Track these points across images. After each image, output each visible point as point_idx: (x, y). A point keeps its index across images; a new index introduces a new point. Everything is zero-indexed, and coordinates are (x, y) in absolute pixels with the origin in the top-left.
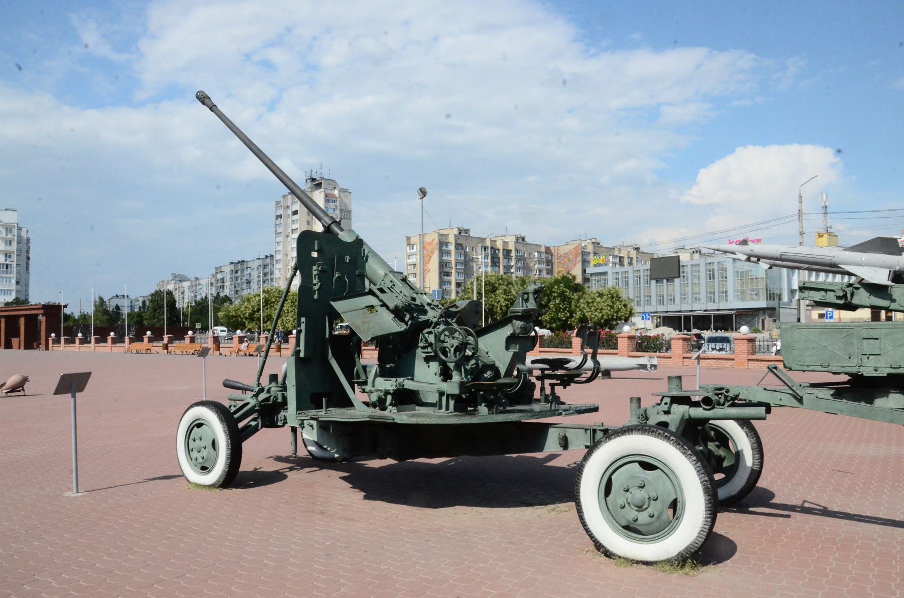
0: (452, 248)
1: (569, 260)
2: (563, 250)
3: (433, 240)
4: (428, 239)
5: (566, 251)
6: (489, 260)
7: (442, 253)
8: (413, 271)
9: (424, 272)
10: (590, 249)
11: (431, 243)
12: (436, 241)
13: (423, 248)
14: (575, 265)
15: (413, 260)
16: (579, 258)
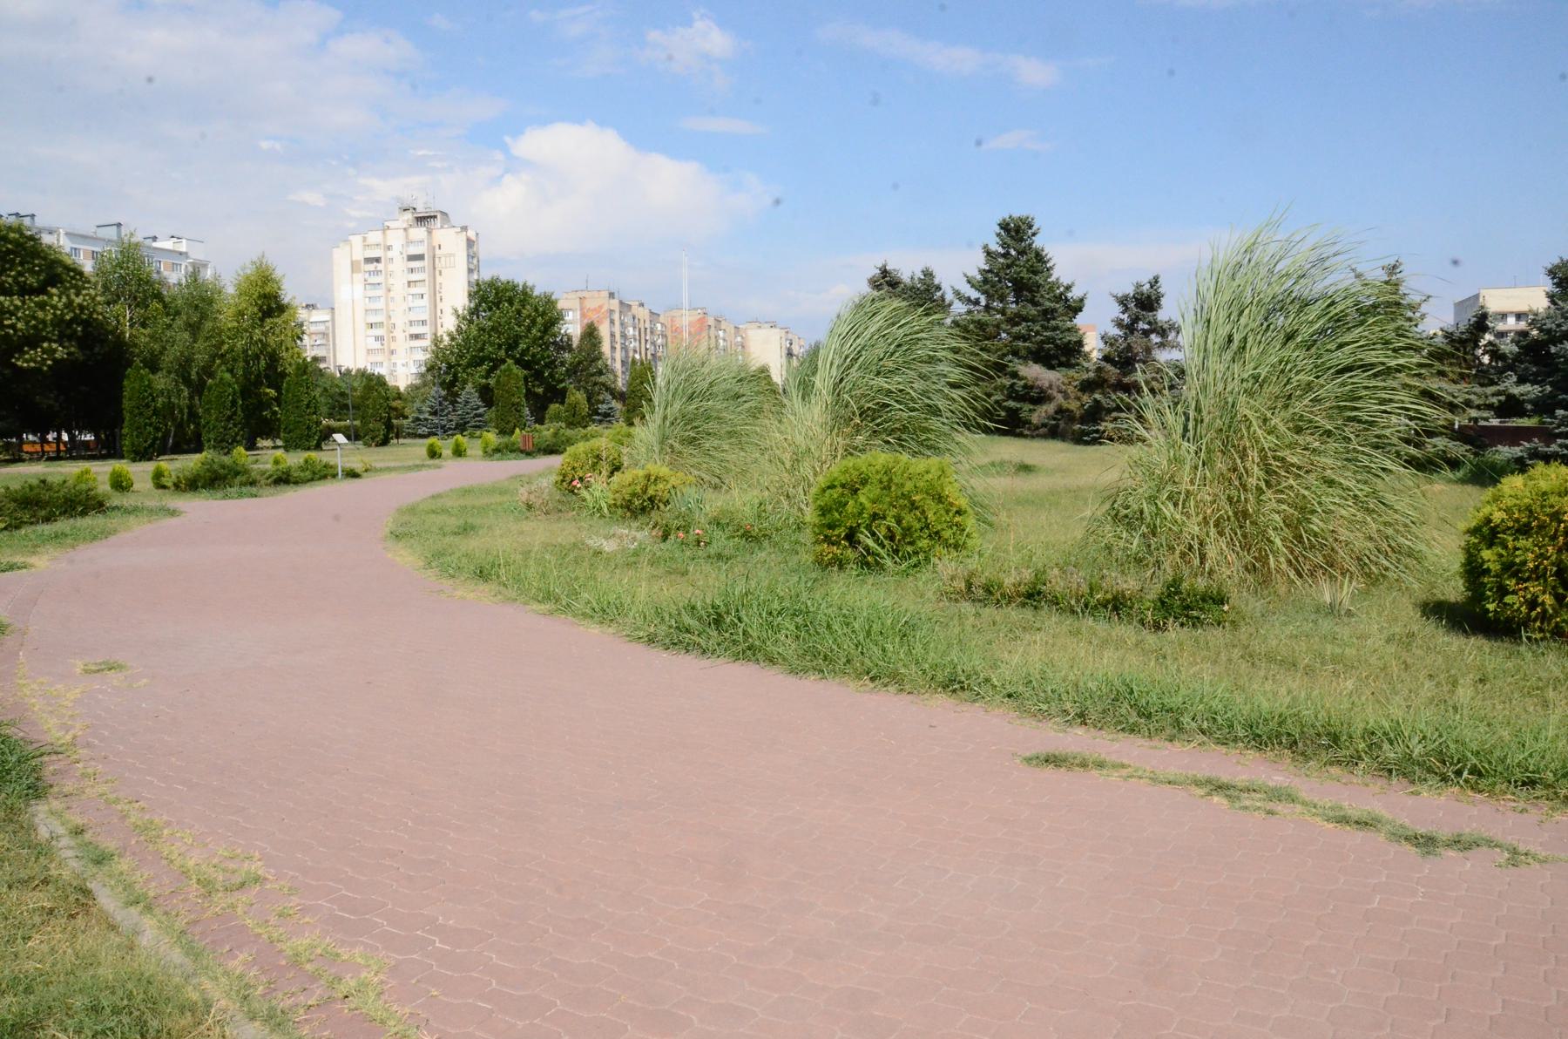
0: (616, 316)
4: (589, 304)
7: (612, 322)
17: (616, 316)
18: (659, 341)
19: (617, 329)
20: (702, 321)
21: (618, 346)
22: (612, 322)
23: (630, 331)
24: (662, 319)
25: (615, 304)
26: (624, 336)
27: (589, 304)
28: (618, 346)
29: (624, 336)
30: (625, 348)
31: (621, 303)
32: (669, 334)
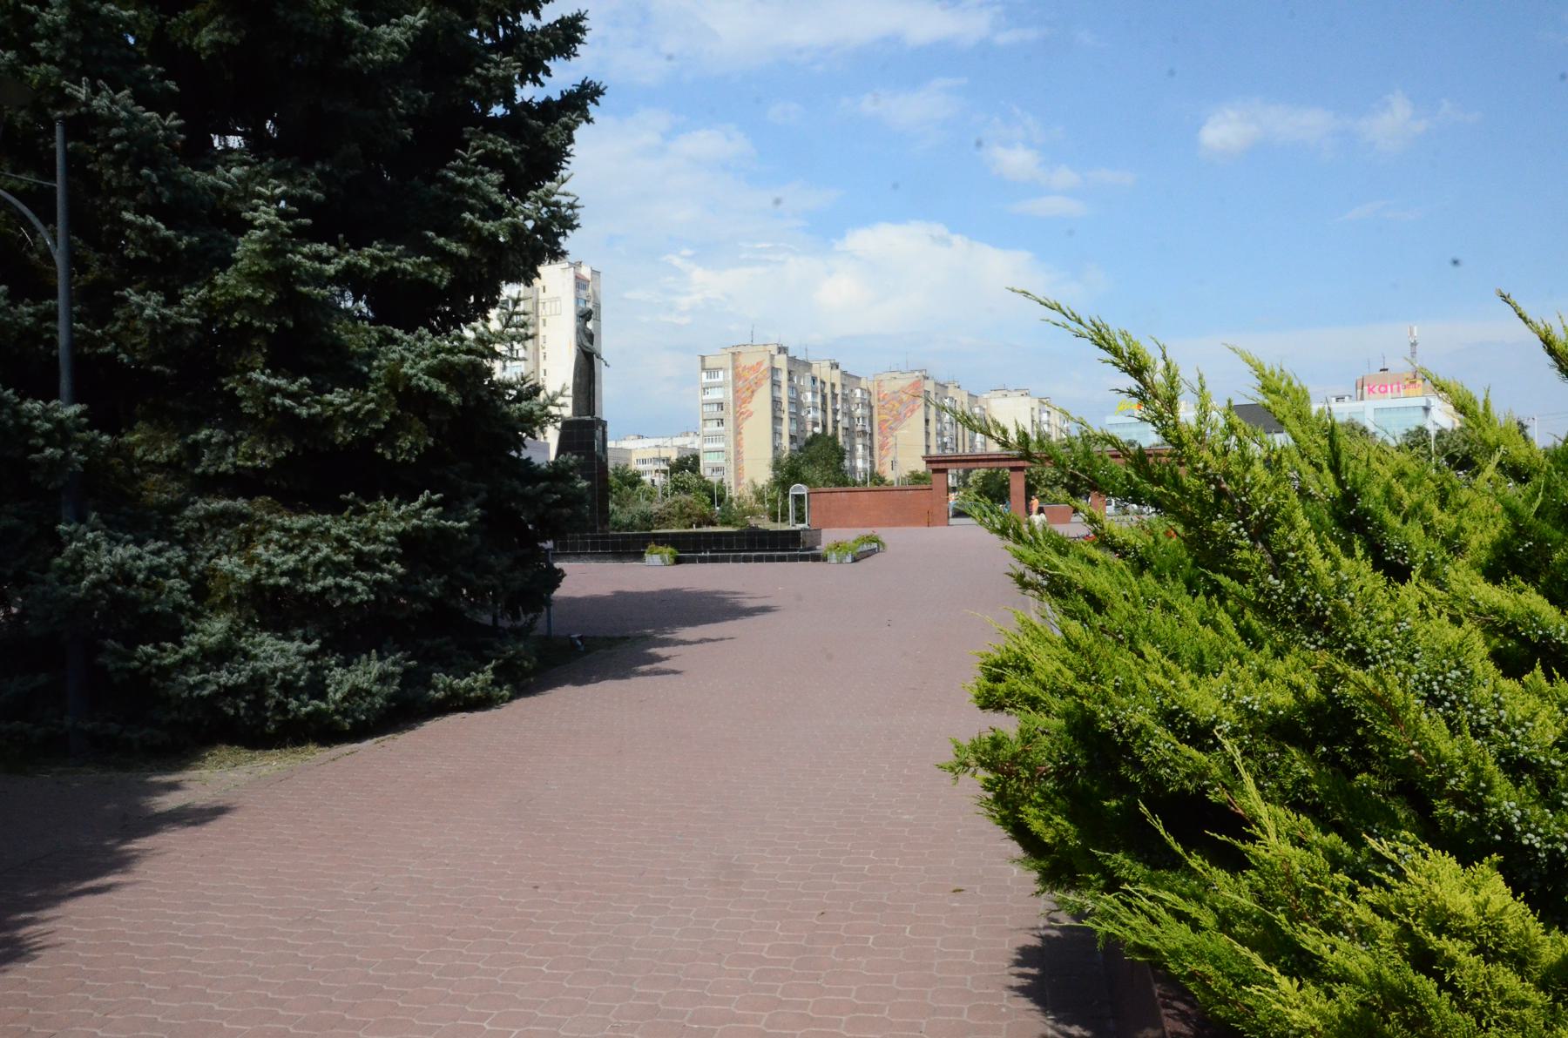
0: (783, 377)
1: (901, 402)
2: (890, 387)
3: (760, 364)
4: (745, 361)
5: (896, 388)
6: (819, 400)
7: (775, 384)
8: (721, 414)
9: (740, 417)
10: (929, 386)
11: (754, 369)
12: (767, 364)
13: (737, 376)
14: (912, 411)
15: (716, 395)
16: (921, 401)
17: (783, 377)
18: (859, 412)
19: (784, 394)
20: (916, 385)
21: (785, 416)
22: (775, 384)
23: (808, 397)
24: (863, 384)
25: (781, 362)
26: (796, 403)
27: (745, 361)
28: (785, 416)
29: (796, 403)
30: (797, 418)
31: (792, 360)
32: (874, 403)
